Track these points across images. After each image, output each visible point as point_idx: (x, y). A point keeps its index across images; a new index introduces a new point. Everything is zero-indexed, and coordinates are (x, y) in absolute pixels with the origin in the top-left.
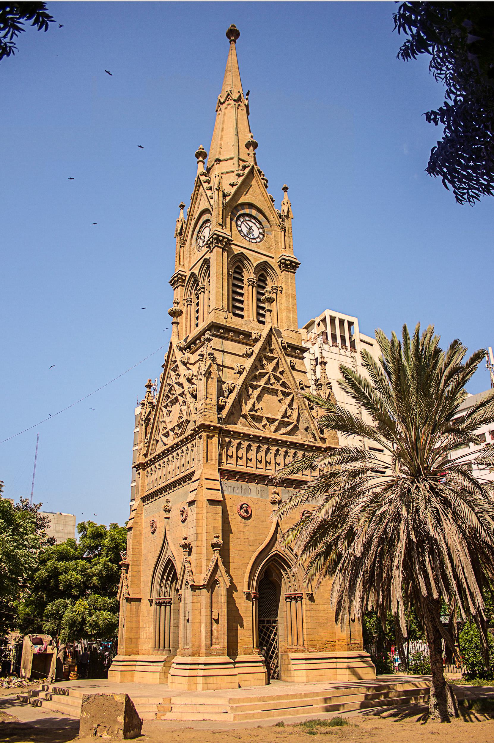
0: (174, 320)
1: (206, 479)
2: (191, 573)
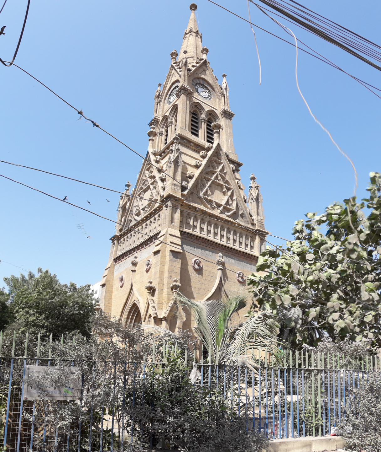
1: (170, 235)
2: (154, 309)
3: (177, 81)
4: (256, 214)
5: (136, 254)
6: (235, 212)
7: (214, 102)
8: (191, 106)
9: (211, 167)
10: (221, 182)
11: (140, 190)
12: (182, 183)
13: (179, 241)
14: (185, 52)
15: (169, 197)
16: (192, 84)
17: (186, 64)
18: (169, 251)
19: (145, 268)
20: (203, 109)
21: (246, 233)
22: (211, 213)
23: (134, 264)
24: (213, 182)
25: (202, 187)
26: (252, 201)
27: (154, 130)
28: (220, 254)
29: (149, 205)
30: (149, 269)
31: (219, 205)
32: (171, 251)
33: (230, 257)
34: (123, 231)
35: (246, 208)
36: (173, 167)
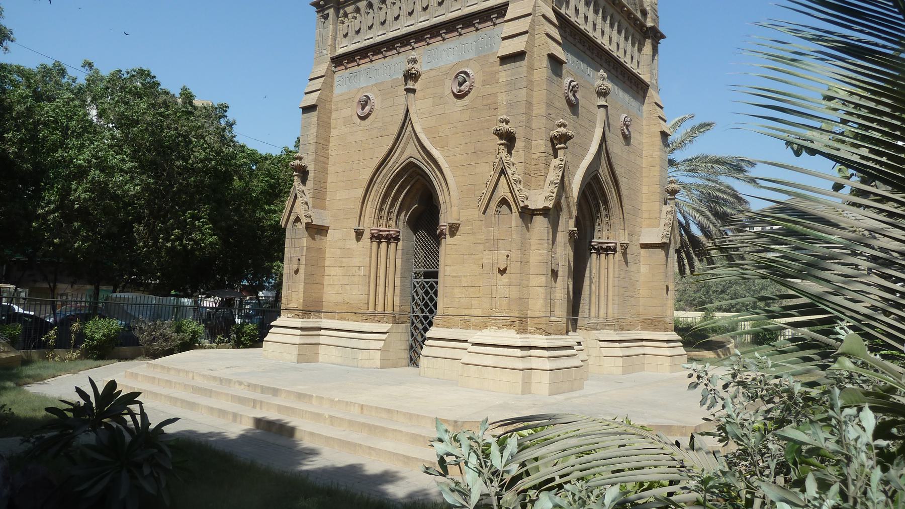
5: (413, 53)
30: (469, 92)
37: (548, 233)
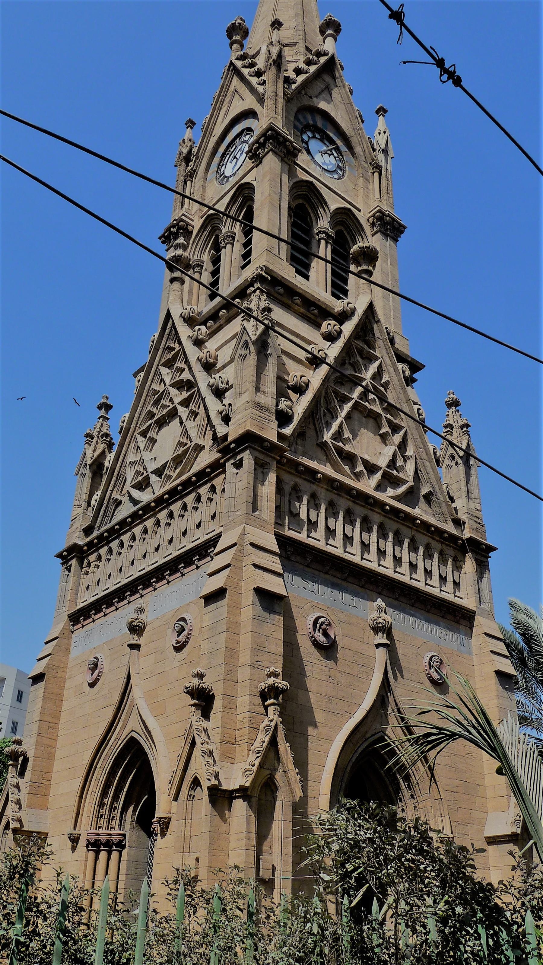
0: (177, 274)
1: (252, 545)
3: (250, 114)
4: (464, 494)
5: (141, 601)
6: (411, 487)
7: (351, 186)
8: (292, 189)
9: (347, 366)
10: (377, 409)
11: (145, 420)
12: (277, 405)
13: (276, 565)
14: (277, 24)
15: (249, 439)
16: (295, 127)
17: (278, 63)
18: (252, 592)
19: (173, 639)
20: (323, 203)
21: (439, 546)
22: (353, 488)
23: (136, 629)
24: (356, 406)
25: (328, 418)
26: (453, 463)
27: (186, 254)
28: (379, 601)
29: (177, 460)
30: (187, 642)
31: (372, 469)
32: (260, 592)
33: (403, 611)
34: (95, 533)
35: (439, 480)
36: (252, 360)
37: (248, 823)
